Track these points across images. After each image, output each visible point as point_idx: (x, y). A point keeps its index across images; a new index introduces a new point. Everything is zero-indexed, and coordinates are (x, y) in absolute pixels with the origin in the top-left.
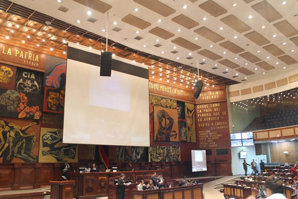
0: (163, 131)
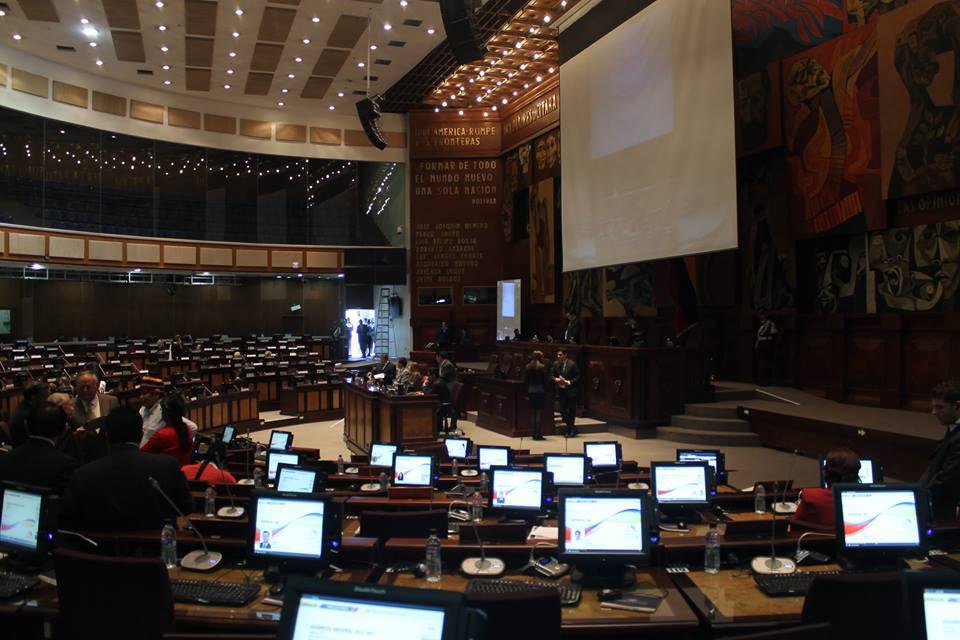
0: (941, 132)
